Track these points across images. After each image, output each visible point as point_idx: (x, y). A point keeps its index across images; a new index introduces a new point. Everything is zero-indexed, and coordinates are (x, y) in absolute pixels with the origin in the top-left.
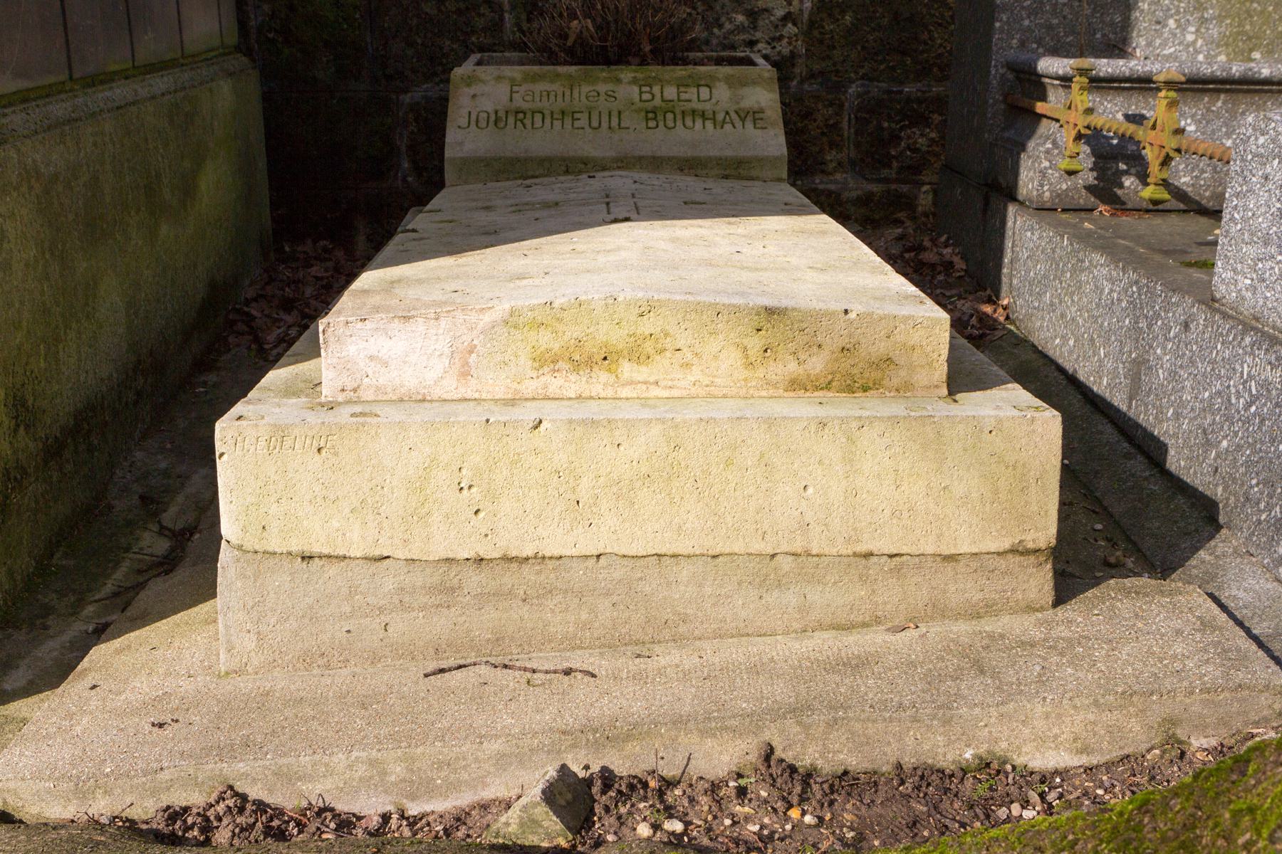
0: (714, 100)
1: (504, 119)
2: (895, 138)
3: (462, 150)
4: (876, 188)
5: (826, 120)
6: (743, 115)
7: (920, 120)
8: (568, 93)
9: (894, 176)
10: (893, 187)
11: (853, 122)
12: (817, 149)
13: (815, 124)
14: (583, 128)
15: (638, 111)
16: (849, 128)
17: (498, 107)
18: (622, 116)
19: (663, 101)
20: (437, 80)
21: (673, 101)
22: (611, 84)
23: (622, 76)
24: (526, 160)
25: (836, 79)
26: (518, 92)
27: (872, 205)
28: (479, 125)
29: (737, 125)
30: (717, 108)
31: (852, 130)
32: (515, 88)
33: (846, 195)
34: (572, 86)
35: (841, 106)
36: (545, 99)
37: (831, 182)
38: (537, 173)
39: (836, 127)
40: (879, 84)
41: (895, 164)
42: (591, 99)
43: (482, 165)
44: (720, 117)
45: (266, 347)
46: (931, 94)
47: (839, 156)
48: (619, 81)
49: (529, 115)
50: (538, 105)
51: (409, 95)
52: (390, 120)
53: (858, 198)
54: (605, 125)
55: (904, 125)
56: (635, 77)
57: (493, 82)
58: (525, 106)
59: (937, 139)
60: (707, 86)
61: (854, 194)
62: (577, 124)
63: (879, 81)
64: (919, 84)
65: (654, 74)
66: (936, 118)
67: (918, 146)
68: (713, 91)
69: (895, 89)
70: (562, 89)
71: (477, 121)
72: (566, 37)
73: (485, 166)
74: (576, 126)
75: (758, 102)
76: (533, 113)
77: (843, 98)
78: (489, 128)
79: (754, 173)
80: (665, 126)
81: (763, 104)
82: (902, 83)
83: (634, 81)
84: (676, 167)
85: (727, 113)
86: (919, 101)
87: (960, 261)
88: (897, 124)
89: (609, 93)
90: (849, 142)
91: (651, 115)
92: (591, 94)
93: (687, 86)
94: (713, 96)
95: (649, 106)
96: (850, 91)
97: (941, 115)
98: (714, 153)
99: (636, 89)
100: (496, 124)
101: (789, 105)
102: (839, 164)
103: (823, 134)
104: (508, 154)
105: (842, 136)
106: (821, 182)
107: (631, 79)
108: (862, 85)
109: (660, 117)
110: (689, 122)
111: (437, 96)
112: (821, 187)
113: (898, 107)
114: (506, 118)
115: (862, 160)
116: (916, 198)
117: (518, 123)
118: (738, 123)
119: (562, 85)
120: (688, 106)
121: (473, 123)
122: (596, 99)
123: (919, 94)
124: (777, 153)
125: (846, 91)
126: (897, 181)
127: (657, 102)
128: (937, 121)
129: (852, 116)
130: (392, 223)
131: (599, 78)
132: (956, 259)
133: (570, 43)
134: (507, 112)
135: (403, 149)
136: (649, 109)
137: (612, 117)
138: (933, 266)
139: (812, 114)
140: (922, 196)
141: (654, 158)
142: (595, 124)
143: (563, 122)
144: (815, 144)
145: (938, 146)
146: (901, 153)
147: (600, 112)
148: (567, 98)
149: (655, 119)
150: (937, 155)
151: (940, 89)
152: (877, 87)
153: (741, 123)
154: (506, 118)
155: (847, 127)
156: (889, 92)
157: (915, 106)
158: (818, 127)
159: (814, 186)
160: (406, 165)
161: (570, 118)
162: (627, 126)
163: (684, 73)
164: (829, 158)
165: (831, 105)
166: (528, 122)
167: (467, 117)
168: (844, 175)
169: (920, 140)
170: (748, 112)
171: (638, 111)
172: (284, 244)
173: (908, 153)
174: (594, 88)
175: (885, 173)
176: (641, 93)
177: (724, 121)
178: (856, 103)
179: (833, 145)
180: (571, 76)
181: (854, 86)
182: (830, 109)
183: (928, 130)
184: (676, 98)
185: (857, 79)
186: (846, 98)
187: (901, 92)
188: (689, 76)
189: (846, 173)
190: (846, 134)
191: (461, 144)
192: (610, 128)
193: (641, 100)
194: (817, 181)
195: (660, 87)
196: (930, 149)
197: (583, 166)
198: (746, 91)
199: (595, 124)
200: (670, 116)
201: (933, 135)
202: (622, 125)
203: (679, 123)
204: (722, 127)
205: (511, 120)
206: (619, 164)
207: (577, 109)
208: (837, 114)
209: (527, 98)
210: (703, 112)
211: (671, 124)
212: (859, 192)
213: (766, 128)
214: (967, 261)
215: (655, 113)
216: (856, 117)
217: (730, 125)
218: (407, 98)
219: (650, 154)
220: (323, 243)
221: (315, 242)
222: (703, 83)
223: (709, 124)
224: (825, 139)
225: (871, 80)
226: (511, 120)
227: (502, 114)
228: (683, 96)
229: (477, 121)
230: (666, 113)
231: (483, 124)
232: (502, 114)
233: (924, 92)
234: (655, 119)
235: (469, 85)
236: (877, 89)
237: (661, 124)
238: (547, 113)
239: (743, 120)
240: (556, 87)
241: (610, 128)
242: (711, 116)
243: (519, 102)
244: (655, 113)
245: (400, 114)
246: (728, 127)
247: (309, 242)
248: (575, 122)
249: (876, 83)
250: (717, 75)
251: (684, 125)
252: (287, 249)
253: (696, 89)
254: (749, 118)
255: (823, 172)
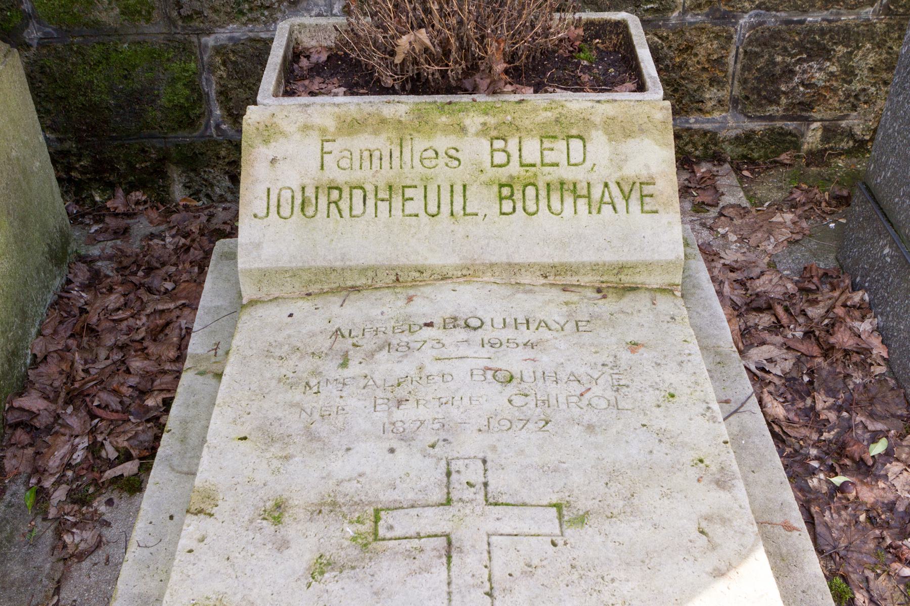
0: (588, 164)
1: (314, 201)
2: (789, 72)
3: (259, 256)
4: (758, 126)
5: (709, 55)
6: (626, 189)
7: (822, 52)
8: (396, 154)
9: (781, 113)
10: (779, 124)
11: (741, 56)
12: (695, 87)
13: (695, 60)
14: (417, 215)
15: (488, 184)
16: (736, 62)
17: (307, 181)
18: (467, 193)
19: (522, 165)
20: (244, 19)
21: (534, 165)
22: (453, 137)
23: (467, 122)
24: (343, 269)
25: (726, 8)
26: (330, 153)
27: (752, 143)
28: (282, 213)
29: (618, 207)
30: (594, 178)
31: (739, 66)
32: (328, 146)
33: (723, 134)
34: (401, 140)
35: (729, 38)
36: (366, 163)
37: (708, 121)
38: (358, 283)
39: (720, 62)
40: (778, 14)
41: (784, 100)
42: (426, 162)
43: (287, 275)
44: (596, 193)
45: (47, 484)
46: (839, 23)
47: (720, 94)
48: (463, 130)
49: (346, 194)
50: (356, 176)
51: (213, 37)
52: (193, 65)
53: (737, 138)
54: (445, 209)
55: (800, 59)
56: (484, 124)
57: (298, 136)
58: (341, 177)
59: (838, 73)
60: (580, 137)
61: (733, 133)
62: (410, 207)
63: (777, 11)
64: (825, 12)
65: (509, 118)
66: (841, 50)
67: (813, 80)
68: (588, 145)
69: (795, 19)
70: (389, 147)
71: (279, 206)
72: (393, 54)
73: (291, 277)
74: (407, 212)
75: (647, 166)
76: (352, 188)
77: (732, 30)
78: (294, 217)
79: (638, 279)
80: (525, 210)
81: (654, 170)
82: (805, 11)
83: (484, 130)
84: (538, 273)
85: (606, 185)
86: (822, 32)
87: (881, 345)
88: (792, 58)
89: (452, 152)
90: (733, 79)
91: (506, 191)
92: (426, 155)
93: (554, 137)
94: (588, 158)
95: (503, 174)
96: (741, 21)
97: (847, 46)
98: (590, 257)
99: (486, 143)
100: (302, 210)
101: (667, 38)
102: (719, 101)
103: (704, 69)
104: (320, 263)
105: (726, 72)
106: (696, 122)
107: (480, 127)
108: (756, 15)
109: (518, 195)
110: (556, 204)
111: (245, 37)
112: (696, 126)
113: (797, 39)
114: (317, 198)
115: (747, 98)
116: (803, 135)
117: (333, 206)
118: (620, 203)
119: (389, 138)
120: (554, 175)
121: (273, 209)
122: (434, 162)
123: (825, 24)
124: (671, 257)
125: (736, 23)
126: (783, 118)
127: (514, 168)
128: (841, 54)
129: (741, 50)
130: (210, 172)
131: (437, 125)
132: (875, 342)
133: (398, 60)
134: (317, 188)
135: (213, 95)
136: (504, 180)
137: (455, 196)
138: (847, 353)
139: (692, 48)
140: (810, 133)
141: (510, 264)
142: (433, 209)
143: (390, 204)
144: (692, 82)
145: (837, 80)
146: (794, 88)
147: (439, 187)
148: (396, 161)
149: (511, 197)
150: (834, 90)
151: (851, 17)
152: (775, 16)
153: (624, 201)
154: (317, 198)
155: (733, 63)
156: (788, 22)
157: (817, 38)
158: (698, 63)
159: (687, 125)
160: (218, 112)
161: (401, 198)
162: (474, 211)
163: (549, 114)
164: (707, 96)
165: (717, 37)
166: (344, 205)
167: (265, 199)
168: (724, 114)
169: (817, 75)
170: (634, 183)
171: (488, 184)
172: (94, 193)
173: (801, 89)
174: (431, 144)
175: (772, 110)
176: (493, 151)
177: (602, 201)
178: (747, 36)
179: (713, 81)
180: (400, 122)
181: (746, 16)
182: (716, 42)
183: (828, 64)
184: (538, 161)
185: (752, 9)
186: (736, 29)
187: (801, 22)
188: (557, 121)
189: (727, 111)
190: (731, 70)
191: (258, 246)
192: (452, 214)
193: (493, 166)
194: (692, 120)
195: (517, 140)
196: (828, 84)
197: (418, 274)
198: (632, 146)
199: (433, 209)
200: (531, 191)
201: (833, 69)
202: (468, 210)
203: (543, 203)
204: (599, 212)
205: (323, 201)
206: (464, 272)
207: (409, 183)
208: (723, 48)
209: (345, 163)
210: (575, 185)
211: (531, 206)
212: (739, 131)
213: (656, 212)
214: (888, 346)
215: (511, 186)
216: (745, 52)
217: (610, 206)
218: (210, 41)
219: (504, 259)
220: (138, 195)
221: (127, 193)
222: (574, 132)
223: (582, 204)
224: (705, 76)
225: (768, 9)
226: (323, 201)
227: (310, 193)
228: (550, 157)
229: (279, 206)
230: (526, 186)
231: (286, 211)
232: (310, 193)
233: (829, 21)
234: (511, 197)
235: (266, 141)
236: (772, 20)
237: (519, 205)
238: (369, 188)
239: (627, 199)
240: (380, 143)
241: (452, 214)
242: (585, 192)
243: (333, 174)
244: (511, 186)
245: (205, 58)
246: (607, 209)
247: (120, 193)
248: (407, 204)
249: (774, 13)
250: (593, 118)
251: (549, 207)
252: (98, 199)
253: (565, 142)
254: (635, 195)
255: (700, 110)
